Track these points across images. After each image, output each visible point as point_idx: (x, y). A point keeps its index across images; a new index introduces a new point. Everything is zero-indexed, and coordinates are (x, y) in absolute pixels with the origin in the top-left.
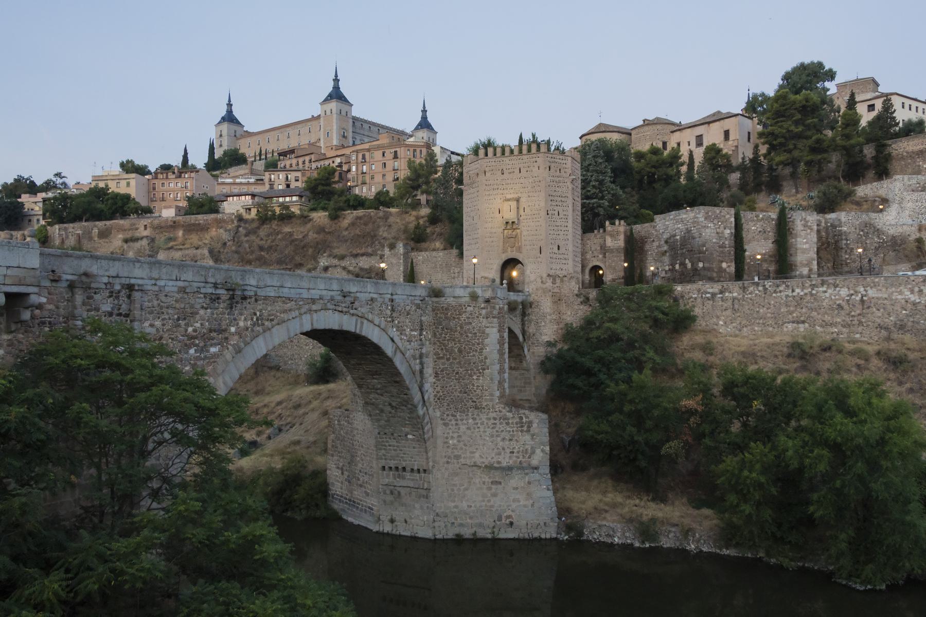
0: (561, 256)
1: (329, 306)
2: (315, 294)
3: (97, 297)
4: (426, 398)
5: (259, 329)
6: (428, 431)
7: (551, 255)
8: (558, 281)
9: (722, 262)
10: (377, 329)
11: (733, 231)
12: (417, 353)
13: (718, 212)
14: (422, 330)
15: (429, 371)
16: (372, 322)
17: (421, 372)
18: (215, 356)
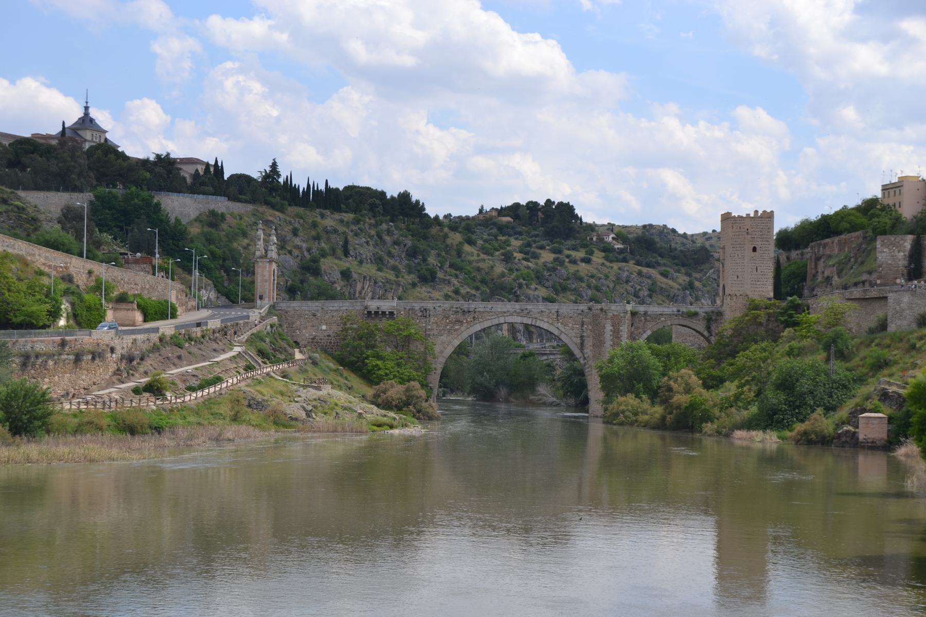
0: (739, 282)
1: (514, 314)
2: (505, 310)
3: (417, 312)
4: (585, 356)
5: (477, 322)
6: (589, 371)
7: (732, 282)
8: (734, 298)
9: (896, 278)
10: (546, 324)
11: (907, 253)
12: (579, 335)
13: (893, 239)
14: (583, 325)
15: (589, 343)
16: (542, 320)
17: (582, 344)
18: (458, 329)
